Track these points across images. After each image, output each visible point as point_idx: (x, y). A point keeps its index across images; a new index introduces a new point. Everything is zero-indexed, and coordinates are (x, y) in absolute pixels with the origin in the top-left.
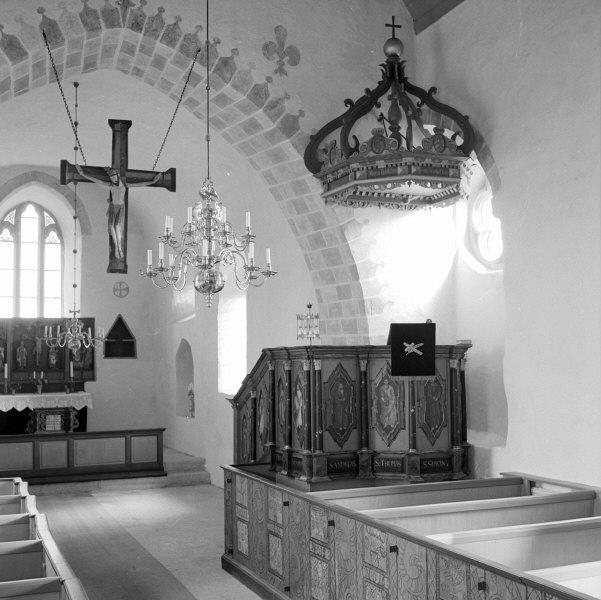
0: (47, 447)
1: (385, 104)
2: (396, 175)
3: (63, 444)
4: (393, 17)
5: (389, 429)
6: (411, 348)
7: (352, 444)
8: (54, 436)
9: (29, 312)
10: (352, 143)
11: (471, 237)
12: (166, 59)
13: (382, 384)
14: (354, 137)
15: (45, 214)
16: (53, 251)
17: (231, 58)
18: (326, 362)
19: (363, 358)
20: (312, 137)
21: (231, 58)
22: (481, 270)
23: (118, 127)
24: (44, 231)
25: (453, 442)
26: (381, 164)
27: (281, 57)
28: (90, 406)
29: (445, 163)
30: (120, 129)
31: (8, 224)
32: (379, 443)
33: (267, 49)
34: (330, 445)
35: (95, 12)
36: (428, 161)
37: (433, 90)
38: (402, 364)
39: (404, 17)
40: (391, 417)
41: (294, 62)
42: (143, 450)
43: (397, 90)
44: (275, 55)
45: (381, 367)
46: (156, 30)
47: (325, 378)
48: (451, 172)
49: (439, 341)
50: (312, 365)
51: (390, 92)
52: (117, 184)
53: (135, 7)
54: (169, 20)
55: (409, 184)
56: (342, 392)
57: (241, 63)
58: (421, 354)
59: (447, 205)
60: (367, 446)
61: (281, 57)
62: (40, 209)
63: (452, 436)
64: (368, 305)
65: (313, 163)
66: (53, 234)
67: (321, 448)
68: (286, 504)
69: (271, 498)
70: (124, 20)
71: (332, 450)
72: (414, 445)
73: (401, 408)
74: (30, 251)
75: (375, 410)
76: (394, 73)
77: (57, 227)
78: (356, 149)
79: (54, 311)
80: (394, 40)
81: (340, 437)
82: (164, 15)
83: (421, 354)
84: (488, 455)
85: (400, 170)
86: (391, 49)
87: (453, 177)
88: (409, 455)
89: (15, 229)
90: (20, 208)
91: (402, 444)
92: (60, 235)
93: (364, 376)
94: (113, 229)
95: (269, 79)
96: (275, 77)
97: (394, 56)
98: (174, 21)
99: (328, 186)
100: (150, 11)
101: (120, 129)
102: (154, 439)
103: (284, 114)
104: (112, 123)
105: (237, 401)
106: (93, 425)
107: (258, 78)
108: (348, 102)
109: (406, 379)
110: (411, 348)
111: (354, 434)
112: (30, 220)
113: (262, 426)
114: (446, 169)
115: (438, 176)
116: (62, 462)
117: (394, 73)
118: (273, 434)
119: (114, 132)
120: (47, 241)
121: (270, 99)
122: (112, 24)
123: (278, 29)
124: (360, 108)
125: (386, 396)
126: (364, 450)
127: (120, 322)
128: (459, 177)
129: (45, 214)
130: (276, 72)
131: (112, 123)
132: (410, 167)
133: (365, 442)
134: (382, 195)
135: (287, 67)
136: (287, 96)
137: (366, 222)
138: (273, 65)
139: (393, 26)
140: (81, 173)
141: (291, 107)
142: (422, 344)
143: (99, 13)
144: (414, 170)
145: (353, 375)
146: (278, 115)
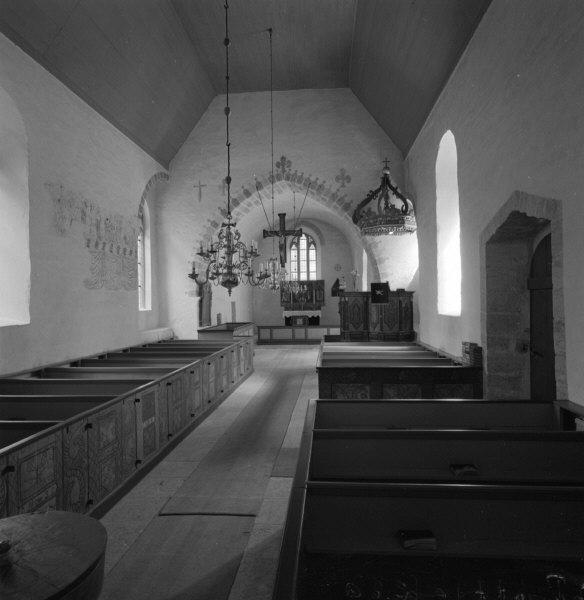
0: (297, 331)
3: (303, 330)
6: (378, 292)
7: (361, 328)
8: (300, 327)
9: (303, 277)
16: (313, 253)
24: (309, 245)
26: (371, 221)
32: (371, 329)
33: (337, 179)
34: (352, 328)
47: (350, 303)
57: (327, 186)
62: (307, 236)
65: (355, 221)
66: (312, 246)
74: (303, 254)
76: (386, 181)
79: (313, 277)
89: (298, 244)
92: (315, 245)
106: (321, 323)
107: (333, 190)
110: (378, 292)
112: (303, 242)
116: (303, 336)
117: (386, 181)
122: (279, 180)
124: (372, 195)
133: (366, 327)
135: (346, 184)
136: (346, 195)
138: (339, 185)
141: (347, 200)
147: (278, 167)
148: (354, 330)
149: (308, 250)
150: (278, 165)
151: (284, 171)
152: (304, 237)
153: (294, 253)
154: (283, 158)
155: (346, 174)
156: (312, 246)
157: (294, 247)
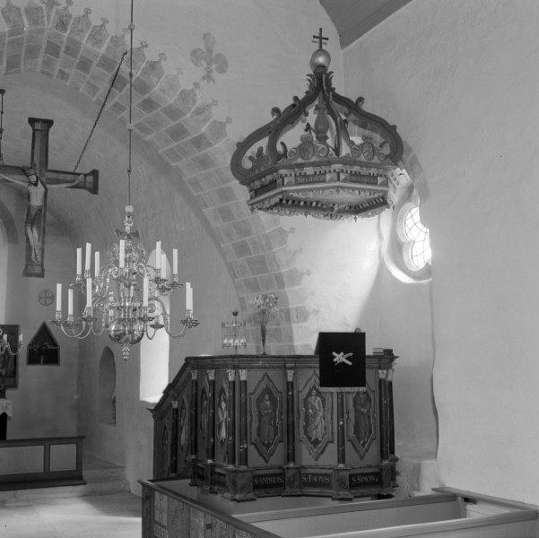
1: (312, 117)
2: (324, 181)
4: (321, 29)
5: (316, 443)
6: (340, 358)
7: (277, 459)
10: (279, 148)
11: (397, 248)
12: (91, 62)
13: (309, 394)
14: (283, 144)
17: (159, 62)
18: (253, 372)
19: (291, 368)
20: (238, 144)
21: (159, 62)
22: (404, 278)
23: (38, 126)
25: (383, 456)
26: (309, 171)
28: (9, 414)
29: (373, 171)
30: (41, 127)
32: (306, 456)
35: (18, 9)
36: (356, 168)
37: (361, 99)
38: (332, 375)
39: (331, 31)
40: (317, 433)
41: (222, 70)
42: (63, 457)
43: (325, 98)
44: (203, 63)
45: (311, 376)
46: (82, 31)
47: (250, 389)
48: (380, 180)
49: (369, 351)
50: (237, 374)
51: (316, 103)
52: (36, 184)
53: (61, 7)
55: (338, 191)
56: (268, 403)
58: (350, 363)
59: (373, 215)
60: (294, 461)
63: (382, 450)
64: (293, 314)
68: (209, 526)
69: (192, 519)
71: (258, 465)
72: (342, 459)
75: (302, 423)
76: (321, 81)
78: (285, 155)
81: (264, 448)
82: (91, 17)
83: (350, 363)
84: (417, 472)
85: (328, 177)
86: (321, 60)
87: (381, 185)
88: (339, 470)
91: (329, 458)
93: (290, 386)
94: (29, 230)
95: (197, 85)
96: (203, 83)
97: (323, 67)
98: (100, 23)
99: (257, 192)
100: (76, 11)
101: (41, 127)
102: (74, 446)
103: (211, 120)
104: (32, 121)
105: (158, 410)
107: (185, 84)
108: (275, 110)
109: (334, 390)
110: (340, 358)
111: (280, 450)
113: (184, 438)
114: (375, 178)
115: (367, 183)
117: (321, 81)
118: (194, 448)
119: (34, 130)
121: (196, 105)
123: (205, 36)
125: (313, 407)
126: (291, 465)
127: (44, 334)
128: (387, 185)
130: (204, 78)
131: (32, 121)
132: (338, 174)
133: (291, 456)
134: (308, 203)
135: (215, 74)
136: (215, 103)
138: (199, 72)
139: (321, 38)
142: (351, 354)
143: (22, 9)
144: (342, 177)
145: (281, 387)
146: (205, 121)
148: (260, 462)
155: (216, 50)
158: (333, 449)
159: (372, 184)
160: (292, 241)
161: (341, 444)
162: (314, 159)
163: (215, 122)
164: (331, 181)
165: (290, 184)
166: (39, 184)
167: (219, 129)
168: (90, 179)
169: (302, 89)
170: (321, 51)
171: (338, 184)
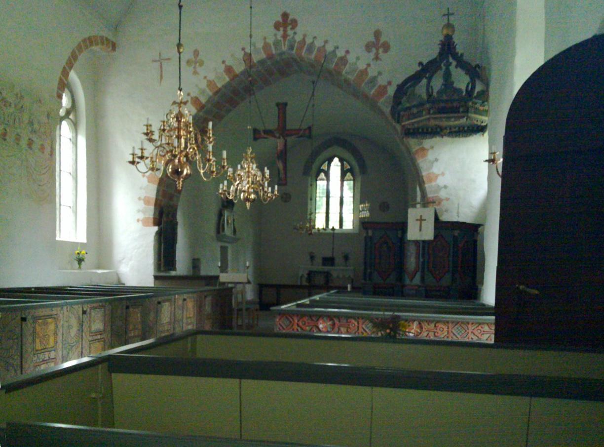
7: (392, 280)
9: (334, 223)
15: (345, 163)
16: (348, 185)
17: (345, 56)
26: (415, 110)
27: (377, 50)
29: (455, 104)
31: (323, 171)
32: (407, 282)
34: (377, 279)
36: (442, 105)
44: (374, 50)
48: (461, 110)
53: (291, 37)
54: (309, 41)
61: (377, 50)
62: (341, 160)
66: (349, 174)
67: (370, 279)
70: (284, 45)
73: (417, 258)
76: (447, 47)
77: (351, 170)
80: (449, 25)
85: (424, 113)
87: (463, 112)
88: (419, 286)
89: (327, 174)
90: (330, 160)
92: (353, 175)
95: (369, 65)
100: (298, 38)
104: (278, 105)
107: (361, 66)
119: (279, 109)
120: (346, 178)
129: (345, 163)
130: (373, 59)
131: (278, 105)
133: (400, 279)
137: (432, 147)
138: (372, 55)
140: (263, 134)
144: (432, 112)
147: (279, 30)
149: (343, 179)
150: (277, 26)
151: (285, 36)
152: (336, 161)
153: (321, 184)
154: (285, 16)
155: (383, 39)
156: (349, 175)
157: (322, 175)
158: (418, 276)
159: (456, 113)
160: (431, 156)
161: (423, 272)
162: (414, 103)
163: (380, 86)
164: (426, 115)
165: (405, 121)
166: (281, 138)
167: (383, 90)
168: (307, 132)
169: (432, 52)
170: (449, 25)
171: (428, 116)
